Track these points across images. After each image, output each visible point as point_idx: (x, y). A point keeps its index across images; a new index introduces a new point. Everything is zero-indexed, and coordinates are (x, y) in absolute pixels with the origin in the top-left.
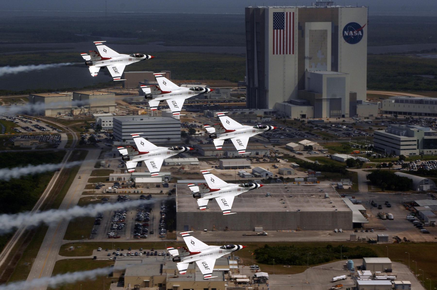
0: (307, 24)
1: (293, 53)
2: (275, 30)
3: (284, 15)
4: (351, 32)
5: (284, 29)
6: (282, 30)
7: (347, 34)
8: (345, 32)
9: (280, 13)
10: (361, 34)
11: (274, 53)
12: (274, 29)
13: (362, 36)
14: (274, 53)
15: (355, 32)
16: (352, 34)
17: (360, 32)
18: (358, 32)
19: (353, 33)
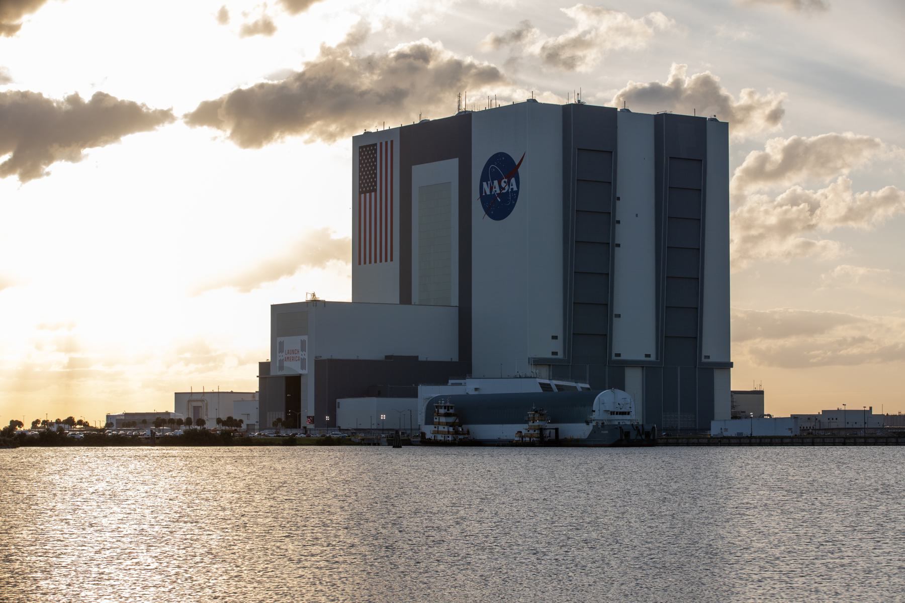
0: (415, 168)
1: (392, 260)
2: (363, 195)
3: (376, 150)
4: (496, 182)
5: (375, 191)
6: (373, 194)
7: (488, 193)
8: (485, 184)
9: (369, 146)
10: (515, 189)
11: (360, 264)
12: (360, 193)
13: (517, 192)
14: (360, 264)
15: (503, 185)
16: (498, 191)
17: (513, 180)
18: (509, 183)
19: (501, 188)
